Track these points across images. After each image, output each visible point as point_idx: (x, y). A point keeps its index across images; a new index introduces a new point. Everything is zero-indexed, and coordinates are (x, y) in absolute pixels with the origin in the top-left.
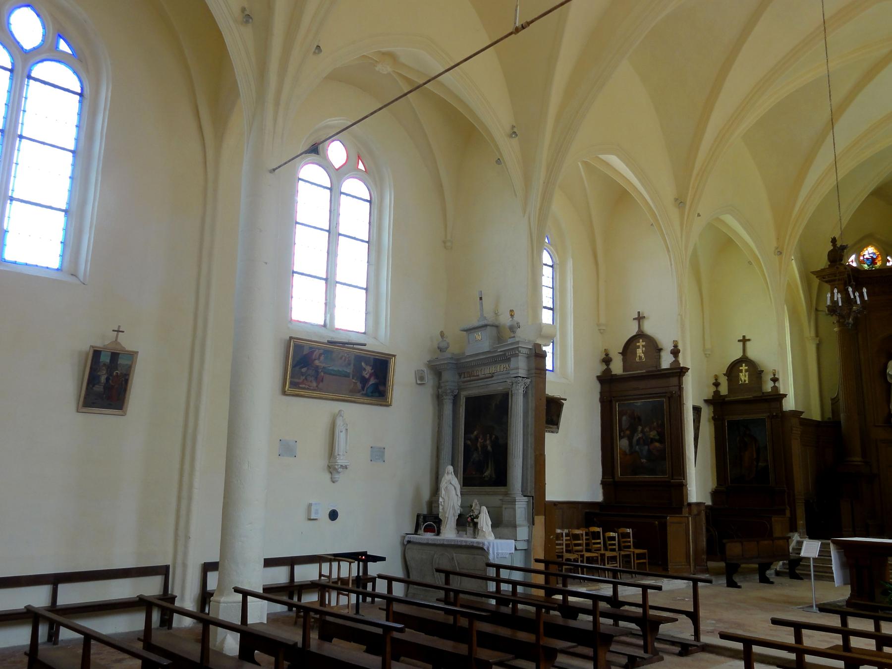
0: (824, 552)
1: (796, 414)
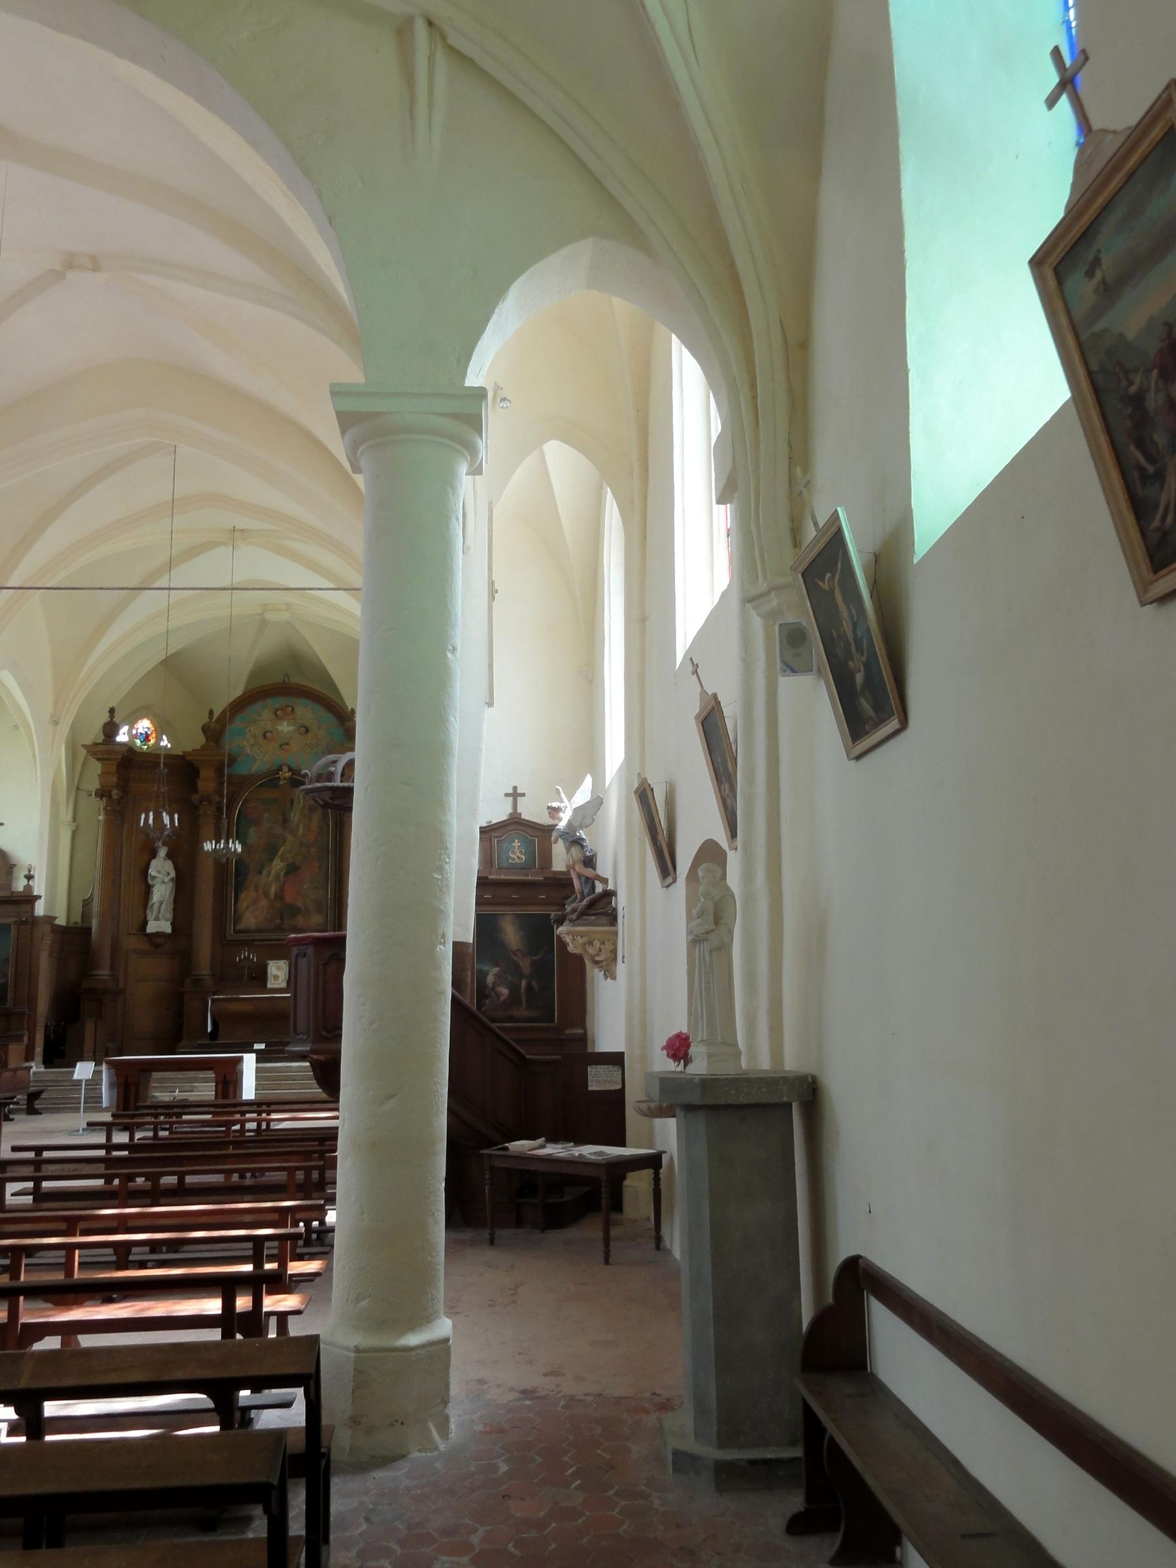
0: (97, 1073)
1: (49, 919)
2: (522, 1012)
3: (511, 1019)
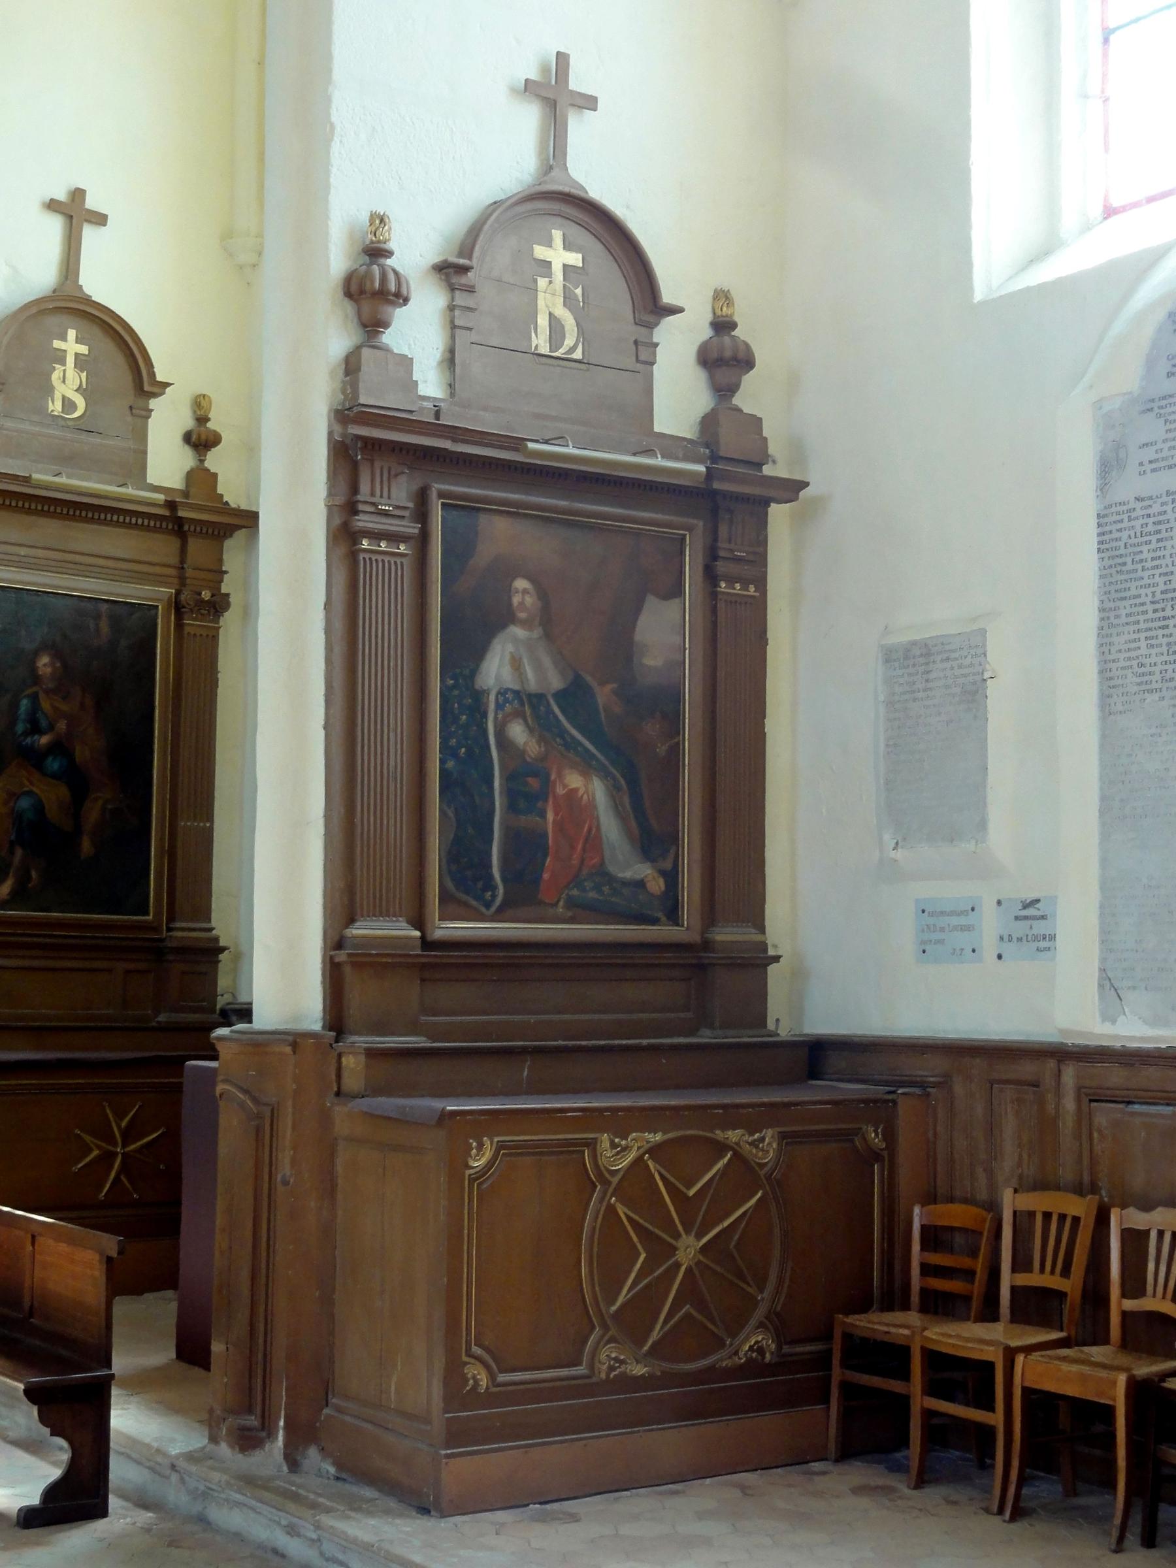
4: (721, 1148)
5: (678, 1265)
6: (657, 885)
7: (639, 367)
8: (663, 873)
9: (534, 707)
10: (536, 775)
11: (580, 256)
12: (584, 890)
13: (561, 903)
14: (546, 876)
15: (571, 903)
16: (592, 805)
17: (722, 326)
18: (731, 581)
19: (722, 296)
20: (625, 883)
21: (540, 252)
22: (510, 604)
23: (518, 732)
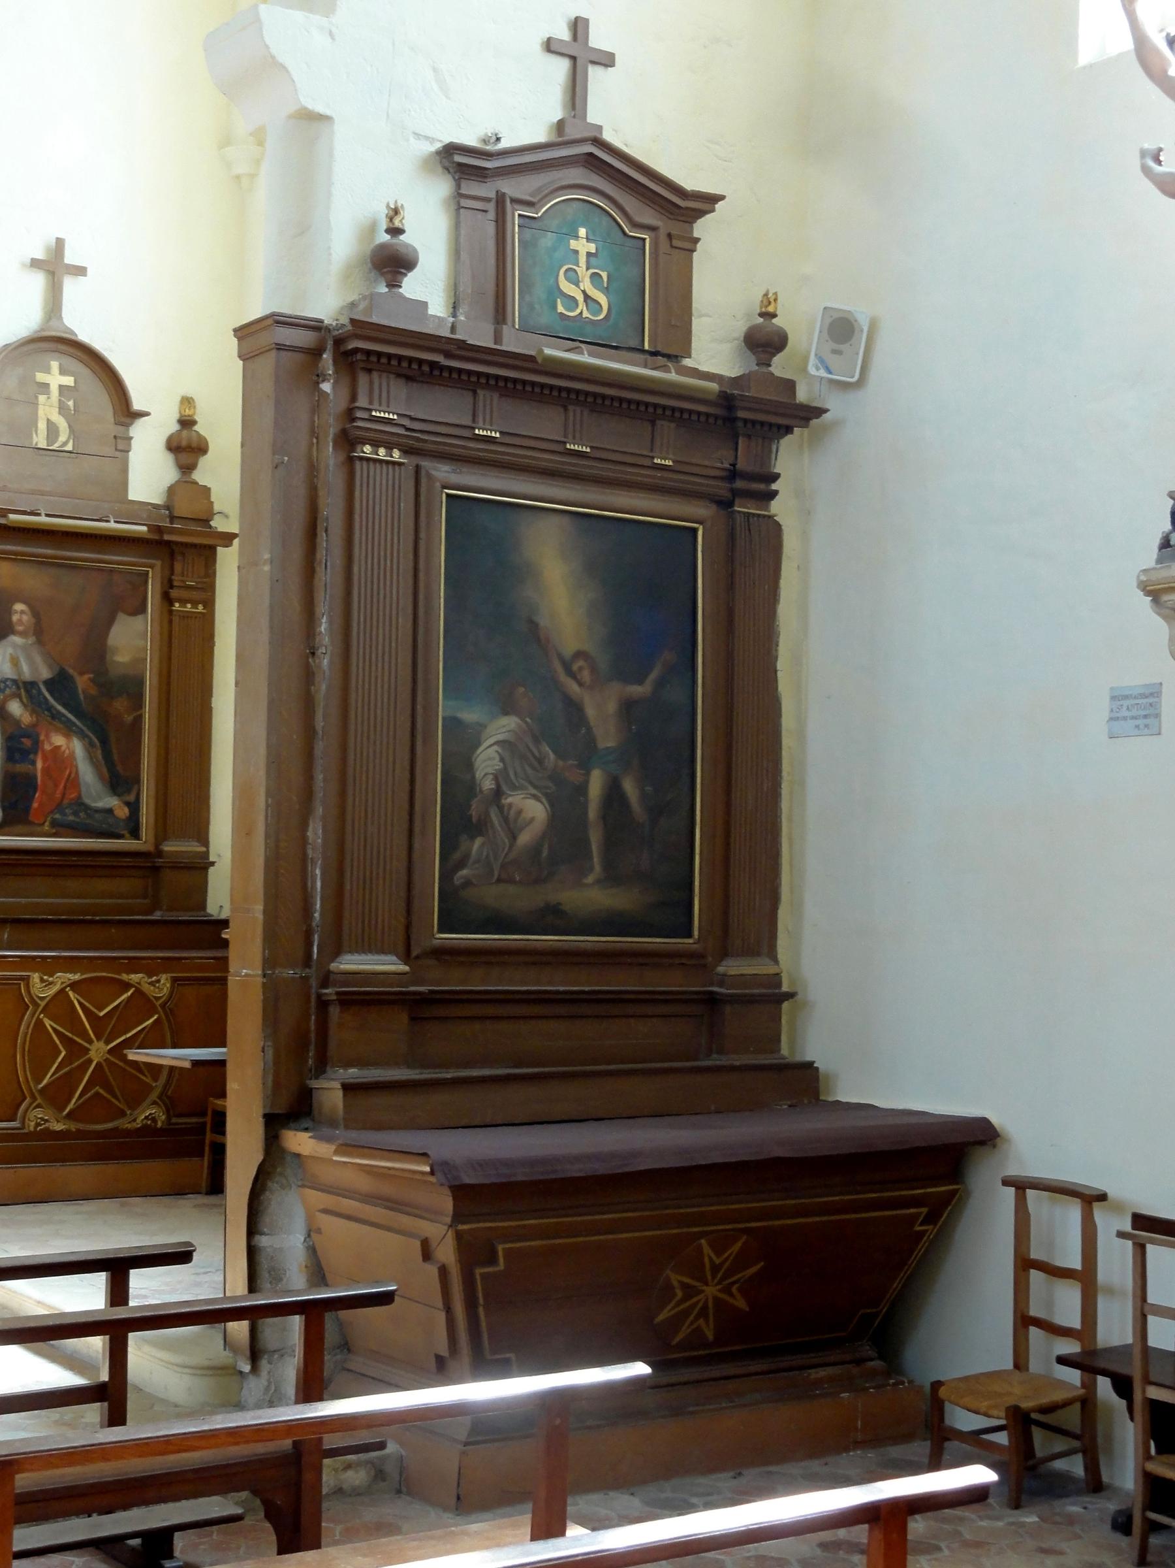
2: (590, 894)
3: (551, 918)
4: (127, 986)
5: (90, 1061)
6: (123, 812)
7: (118, 454)
8: (128, 804)
9: (27, 691)
10: (28, 737)
11: (72, 379)
12: (65, 815)
13: (47, 823)
14: (35, 805)
15: (54, 824)
16: (72, 755)
17: (186, 423)
18: (183, 602)
19: (187, 401)
20: (97, 811)
21: (41, 377)
22: (11, 621)
23: (15, 708)
